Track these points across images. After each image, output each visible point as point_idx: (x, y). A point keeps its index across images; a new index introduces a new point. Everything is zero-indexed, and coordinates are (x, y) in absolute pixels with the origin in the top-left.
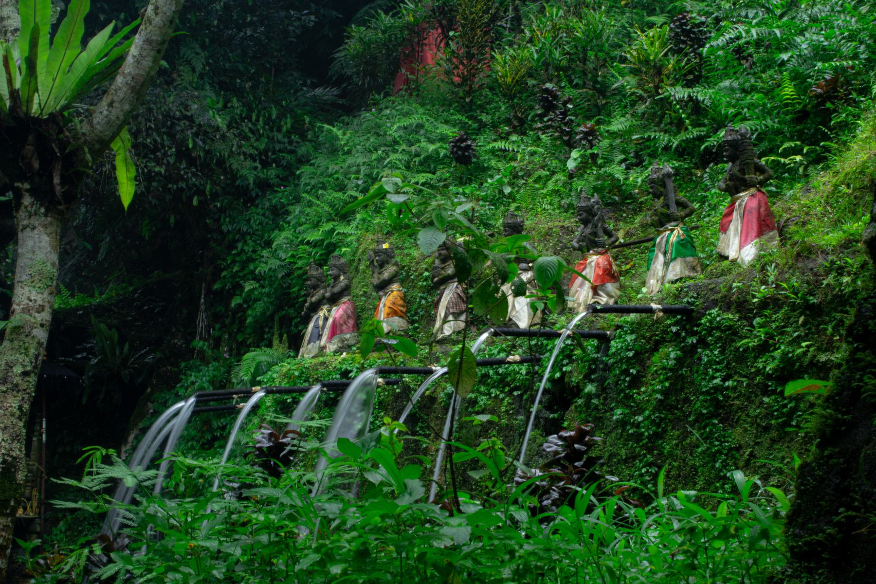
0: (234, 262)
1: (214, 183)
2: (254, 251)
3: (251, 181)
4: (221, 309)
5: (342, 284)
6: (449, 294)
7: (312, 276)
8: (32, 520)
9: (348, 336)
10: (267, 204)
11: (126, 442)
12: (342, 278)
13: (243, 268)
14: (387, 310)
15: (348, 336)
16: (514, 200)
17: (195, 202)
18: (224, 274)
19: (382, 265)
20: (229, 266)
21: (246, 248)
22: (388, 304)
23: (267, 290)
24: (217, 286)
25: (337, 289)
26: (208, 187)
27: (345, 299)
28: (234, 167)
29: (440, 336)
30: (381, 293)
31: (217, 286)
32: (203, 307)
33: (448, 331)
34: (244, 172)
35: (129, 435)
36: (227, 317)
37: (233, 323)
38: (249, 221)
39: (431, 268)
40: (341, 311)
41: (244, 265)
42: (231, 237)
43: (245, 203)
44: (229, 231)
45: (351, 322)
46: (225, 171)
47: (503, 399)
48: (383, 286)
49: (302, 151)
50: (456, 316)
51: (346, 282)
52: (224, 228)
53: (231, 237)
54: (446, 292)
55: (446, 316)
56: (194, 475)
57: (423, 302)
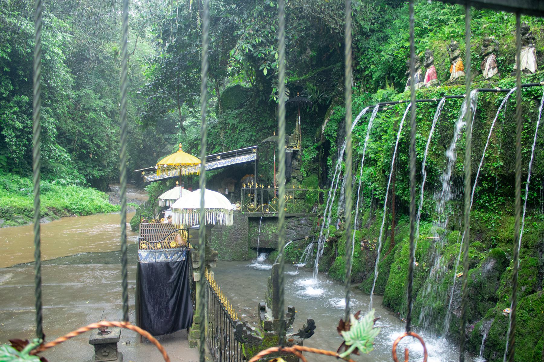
0: (364, 59)
2: (373, 54)
4: (358, 76)
5: (431, 60)
6: (490, 59)
8: (298, 151)
9: (434, 80)
11: (324, 124)
12: (431, 57)
13: (368, 61)
14: (457, 69)
15: (434, 80)
16: (509, 22)
18: (360, 63)
19: (453, 51)
21: (370, 53)
22: (457, 66)
23: (379, 68)
25: (429, 62)
28: (362, 24)
29: (487, 78)
30: (453, 62)
31: (358, 68)
33: (490, 75)
34: (366, 26)
36: (362, 79)
37: (364, 81)
38: (369, 43)
39: (477, 50)
40: (431, 71)
42: (362, 49)
43: (366, 38)
45: (435, 75)
47: (530, 102)
48: (455, 59)
49: (387, 17)
50: (493, 68)
53: (362, 49)
54: (488, 59)
55: (489, 69)
56: (357, 135)
57: (472, 65)
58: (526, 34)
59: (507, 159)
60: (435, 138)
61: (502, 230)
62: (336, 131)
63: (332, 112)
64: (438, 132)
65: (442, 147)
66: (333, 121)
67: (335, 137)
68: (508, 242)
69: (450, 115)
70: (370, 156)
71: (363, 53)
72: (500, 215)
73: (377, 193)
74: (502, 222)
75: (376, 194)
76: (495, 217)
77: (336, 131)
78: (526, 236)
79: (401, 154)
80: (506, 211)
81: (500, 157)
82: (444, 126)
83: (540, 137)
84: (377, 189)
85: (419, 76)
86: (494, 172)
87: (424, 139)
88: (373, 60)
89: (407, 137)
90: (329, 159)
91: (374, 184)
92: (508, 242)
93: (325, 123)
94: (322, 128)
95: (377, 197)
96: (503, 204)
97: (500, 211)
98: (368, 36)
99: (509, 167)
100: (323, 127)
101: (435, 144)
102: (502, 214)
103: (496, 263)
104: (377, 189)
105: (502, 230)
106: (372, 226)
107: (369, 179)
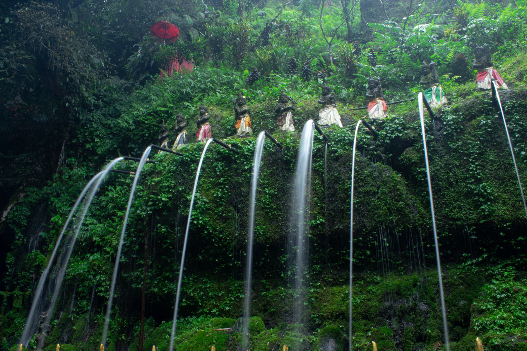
1: (75, 101)
3: (93, 103)
7: (180, 116)
10: (100, 112)
11: (6, 209)
12: (206, 114)
14: (247, 123)
17: (67, 105)
20: (81, 133)
24: (74, 141)
26: (73, 101)
27: (207, 123)
31: (74, 141)
32: (63, 150)
34: (89, 99)
35: (8, 206)
38: (93, 117)
41: (91, 133)
44: (82, 120)
46: (79, 97)
51: (208, 116)
52: (81, 118)
53: (83, 122)
58: (328, 94)
59: (330, 214)
60: (224, 198)
61: (325, 304)
62: (27, 217)
63: (22, 195)
64: (227, 189)
65: (232, 208)
66: (24, 205)
67: (25, 226)
68: (337, 317)
69: (246, 168)
70: (94, 239)
71: (83, 126)
72: (316, 287)
73: (103, 289)
74: (322, 295)
75: (101, 291)
76: (312, 290)
77: (27, 217)
78: (362, 304)
79: (159, 225)
80: (324, 281)
81: (319, 213)
82: (237, 182)
83: (372, 186)
84: (104, 284)
85: (184, 136)
86: (311, 232)
87: (205, 200)
88: (98, 132)
89: (175, 200)
90: (9, 255)
91: (98, 278)
92: (337, 317)
93: (9, 208)
94: (2, 213)
95: (102, 294)
96: (320, 273)
97: (316, 282)
98: (90, 111)
99: (333, 223)
100: (5, 214)
101: (221, 205)
102: (320, 286)
103: (336, 342)
104: (104, 284)
105: (325, 304)
106: (92, 338)
107: (88, 271)
